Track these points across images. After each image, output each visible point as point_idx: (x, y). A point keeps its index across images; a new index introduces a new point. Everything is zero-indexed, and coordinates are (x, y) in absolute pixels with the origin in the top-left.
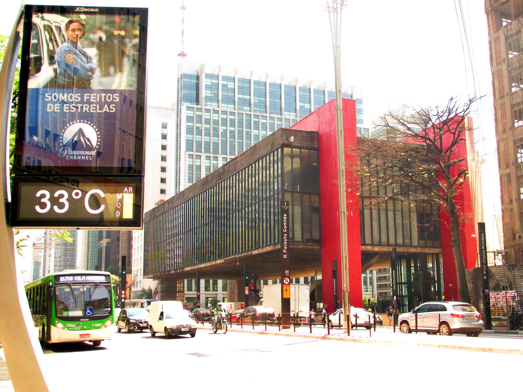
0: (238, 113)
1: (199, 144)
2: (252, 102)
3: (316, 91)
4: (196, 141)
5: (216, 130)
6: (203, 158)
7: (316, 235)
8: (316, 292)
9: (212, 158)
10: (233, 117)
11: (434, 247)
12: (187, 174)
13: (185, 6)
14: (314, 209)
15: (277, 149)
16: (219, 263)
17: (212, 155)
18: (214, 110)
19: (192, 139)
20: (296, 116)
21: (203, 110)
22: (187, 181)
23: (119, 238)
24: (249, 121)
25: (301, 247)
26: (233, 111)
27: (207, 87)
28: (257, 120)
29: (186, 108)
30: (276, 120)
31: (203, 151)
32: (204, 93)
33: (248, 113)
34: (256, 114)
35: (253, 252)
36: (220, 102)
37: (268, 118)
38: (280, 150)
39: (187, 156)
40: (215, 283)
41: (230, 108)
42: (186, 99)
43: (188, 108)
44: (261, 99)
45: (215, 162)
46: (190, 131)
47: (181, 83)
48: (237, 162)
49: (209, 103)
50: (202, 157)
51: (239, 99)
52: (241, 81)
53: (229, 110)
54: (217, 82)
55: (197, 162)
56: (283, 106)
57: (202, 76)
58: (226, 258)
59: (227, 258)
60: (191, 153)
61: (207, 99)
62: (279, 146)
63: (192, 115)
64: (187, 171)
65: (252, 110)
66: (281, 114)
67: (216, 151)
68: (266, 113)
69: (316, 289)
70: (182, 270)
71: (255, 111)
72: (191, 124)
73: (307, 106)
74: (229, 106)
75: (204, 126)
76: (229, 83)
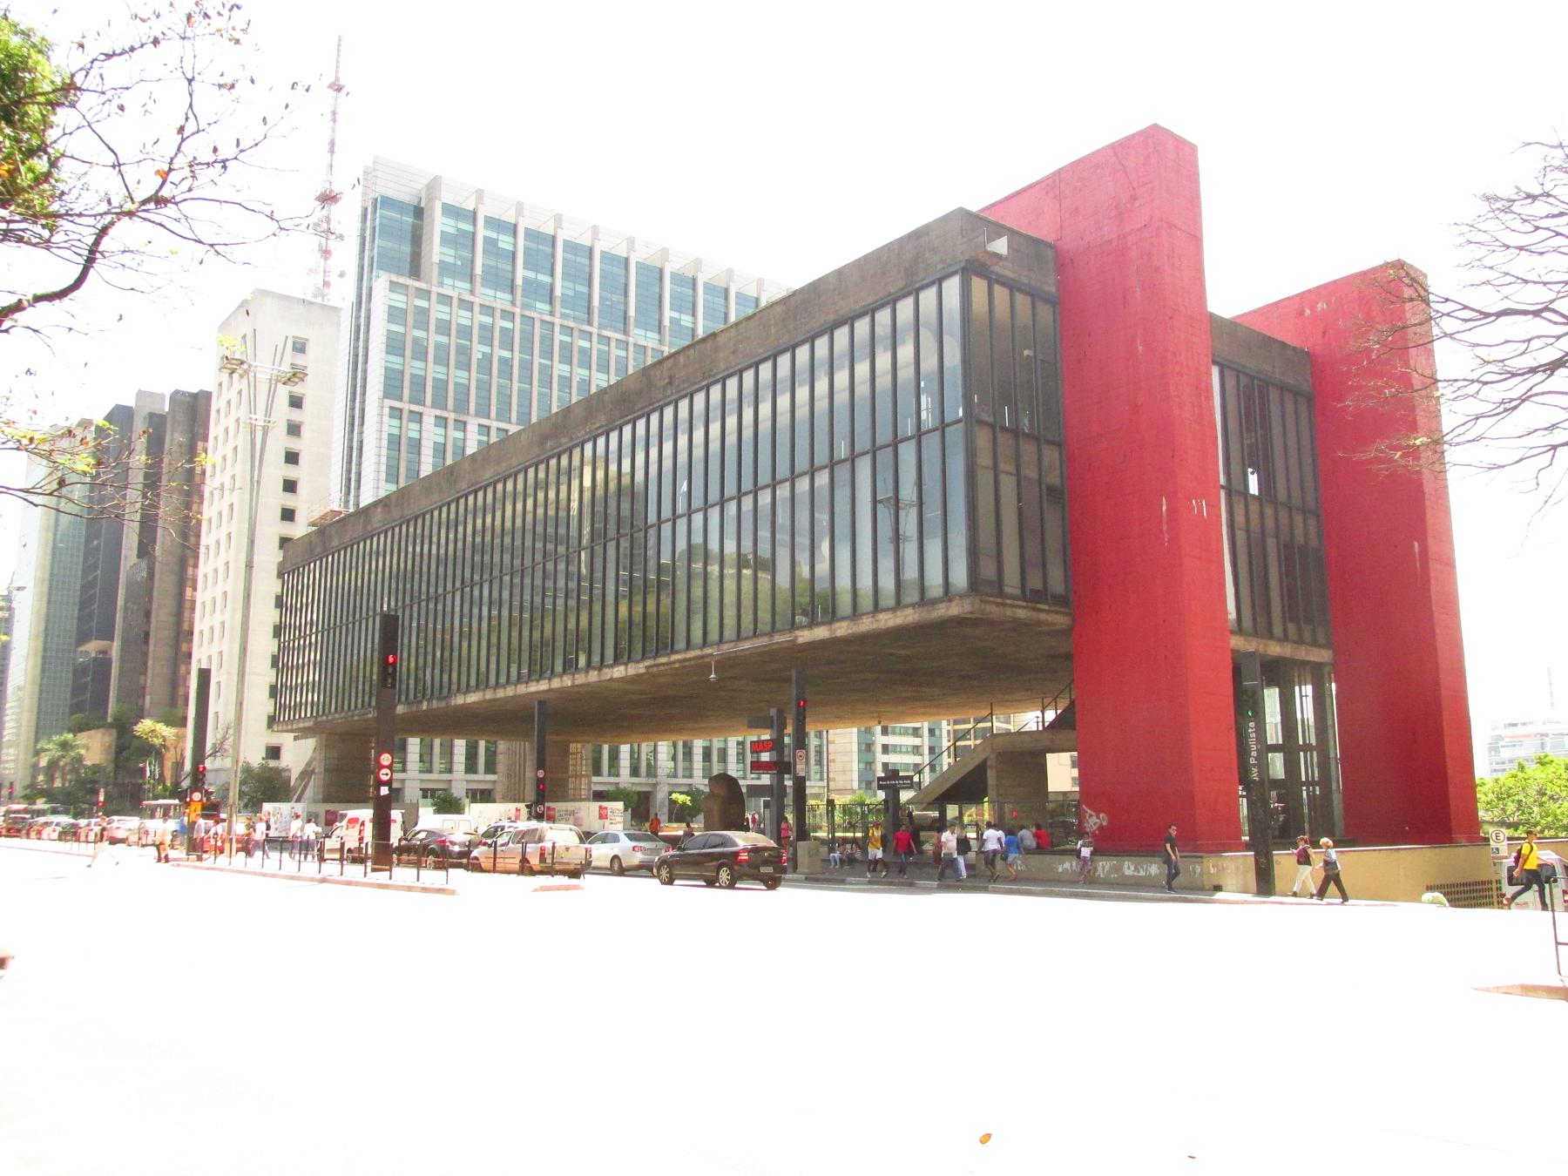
0: (522, 316)
1: (419, 383)
2: (558, 292)
3: (708, 287)
4: (411, 374)
5: (465, 353)
6: (429, 420)
7: (1057, 583)
8: (991, 776)
9: (451, 424)
10: (509, 325)
11: (1314, 643)
12: (384, 460)
13: (342, 82)
14: (1054, 493)
17: (452, 416)
18: (461, 300)
19: (401, 368)
20: (661, 342)
21: (434, 297)
22: (383, 476)
23: (147, 635)
24: (548, 341)
26: (509, 308)
27: (446, 239)
28: (568, 339)
29: (387, 285)
30: (613, 344)
31: (429, 401)
32: (436, 252)
33: (548, 318)
34: (566, 323)
35: (798, 633)
36: (478, 280)
37: (595, 338)
38: (952, 287)
39: (386, 411)
40: (448, 753)
41: (501, 300)
42: (387, 262)
43: (394, 286)
44: (579, 288)
45: (459, 435)
46: (395, 345)
47: (374, 220)
48: (716, 349)
49: (448, 281)
50: (424, 417)
51: (525, 280)
52: (532, 235)
53: (498, 305)
54: (469, 228)
55: (412, 430)
56: (632, 312)
57: (432, 209)
58: (657, 656)
59: (663, 660)
60: (397, 404)
61: (445, 268)
63: (404, 306)
64: (384, 451)
65: (558, 314)
66: (626, 332)
67: (461, 407)
68: (590, 323)
70: (443, 704)
71: (563, 316)
72: (400, 329)
73: (686, 320)
74: (499, 294)
75: (435, 338)
76: (502, 237)
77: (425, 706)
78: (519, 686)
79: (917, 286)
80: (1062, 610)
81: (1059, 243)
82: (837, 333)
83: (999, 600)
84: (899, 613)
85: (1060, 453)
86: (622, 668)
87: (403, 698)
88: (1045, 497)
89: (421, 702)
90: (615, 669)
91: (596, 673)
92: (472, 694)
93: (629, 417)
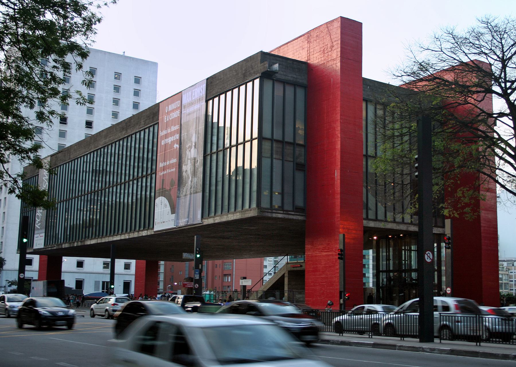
7: (300, 202)
15: (253, 81)
16: (144, 235)
25: (280, 216)
38: (257, 82)
62: (257, 76)
69: (286, 275)
77: (75, 245)
78: (110, 237)
79: (246, 81)
80: (301, 214)
81: (309, 62)
82: (241, 87)
83: (270, 211)
84: (235, 215)
85: (305, 150)
86: (146, 231)
87: (68, 241)
88: (295, 168)
89: (74, 243)
90: (144, 232)
91: (137, 233)
92: (93, 240)
93: (152, 124)
